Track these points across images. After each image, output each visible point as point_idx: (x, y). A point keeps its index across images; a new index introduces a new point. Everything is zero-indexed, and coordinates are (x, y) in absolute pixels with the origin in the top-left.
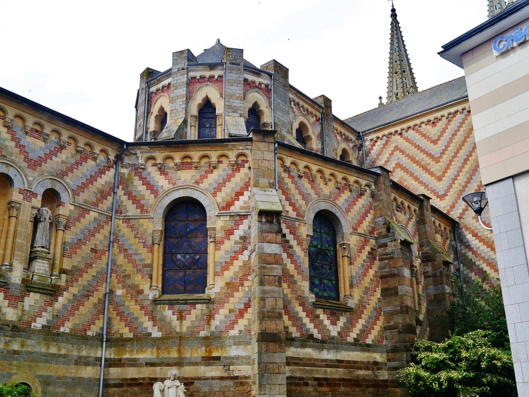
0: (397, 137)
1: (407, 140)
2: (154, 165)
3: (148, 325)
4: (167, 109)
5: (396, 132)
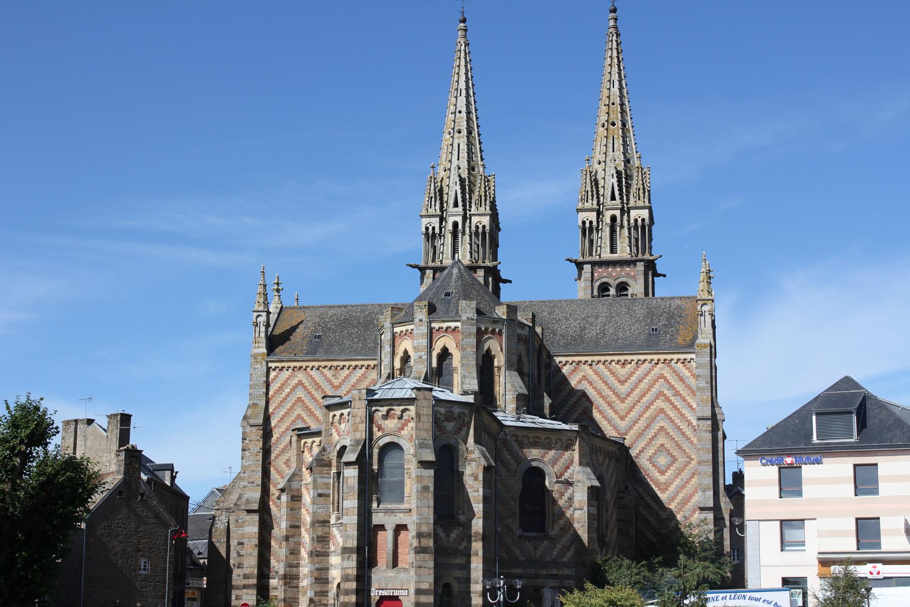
0: (587, 367)
1: (596, 373)
2: (515, 441)
3: (517, 552)
4: (452, 349)
5: (586, 362)
